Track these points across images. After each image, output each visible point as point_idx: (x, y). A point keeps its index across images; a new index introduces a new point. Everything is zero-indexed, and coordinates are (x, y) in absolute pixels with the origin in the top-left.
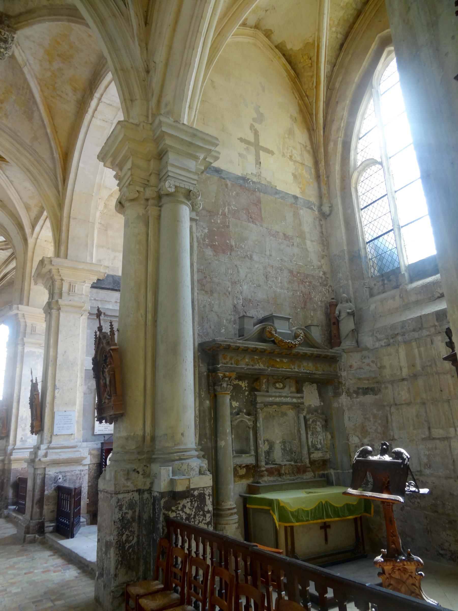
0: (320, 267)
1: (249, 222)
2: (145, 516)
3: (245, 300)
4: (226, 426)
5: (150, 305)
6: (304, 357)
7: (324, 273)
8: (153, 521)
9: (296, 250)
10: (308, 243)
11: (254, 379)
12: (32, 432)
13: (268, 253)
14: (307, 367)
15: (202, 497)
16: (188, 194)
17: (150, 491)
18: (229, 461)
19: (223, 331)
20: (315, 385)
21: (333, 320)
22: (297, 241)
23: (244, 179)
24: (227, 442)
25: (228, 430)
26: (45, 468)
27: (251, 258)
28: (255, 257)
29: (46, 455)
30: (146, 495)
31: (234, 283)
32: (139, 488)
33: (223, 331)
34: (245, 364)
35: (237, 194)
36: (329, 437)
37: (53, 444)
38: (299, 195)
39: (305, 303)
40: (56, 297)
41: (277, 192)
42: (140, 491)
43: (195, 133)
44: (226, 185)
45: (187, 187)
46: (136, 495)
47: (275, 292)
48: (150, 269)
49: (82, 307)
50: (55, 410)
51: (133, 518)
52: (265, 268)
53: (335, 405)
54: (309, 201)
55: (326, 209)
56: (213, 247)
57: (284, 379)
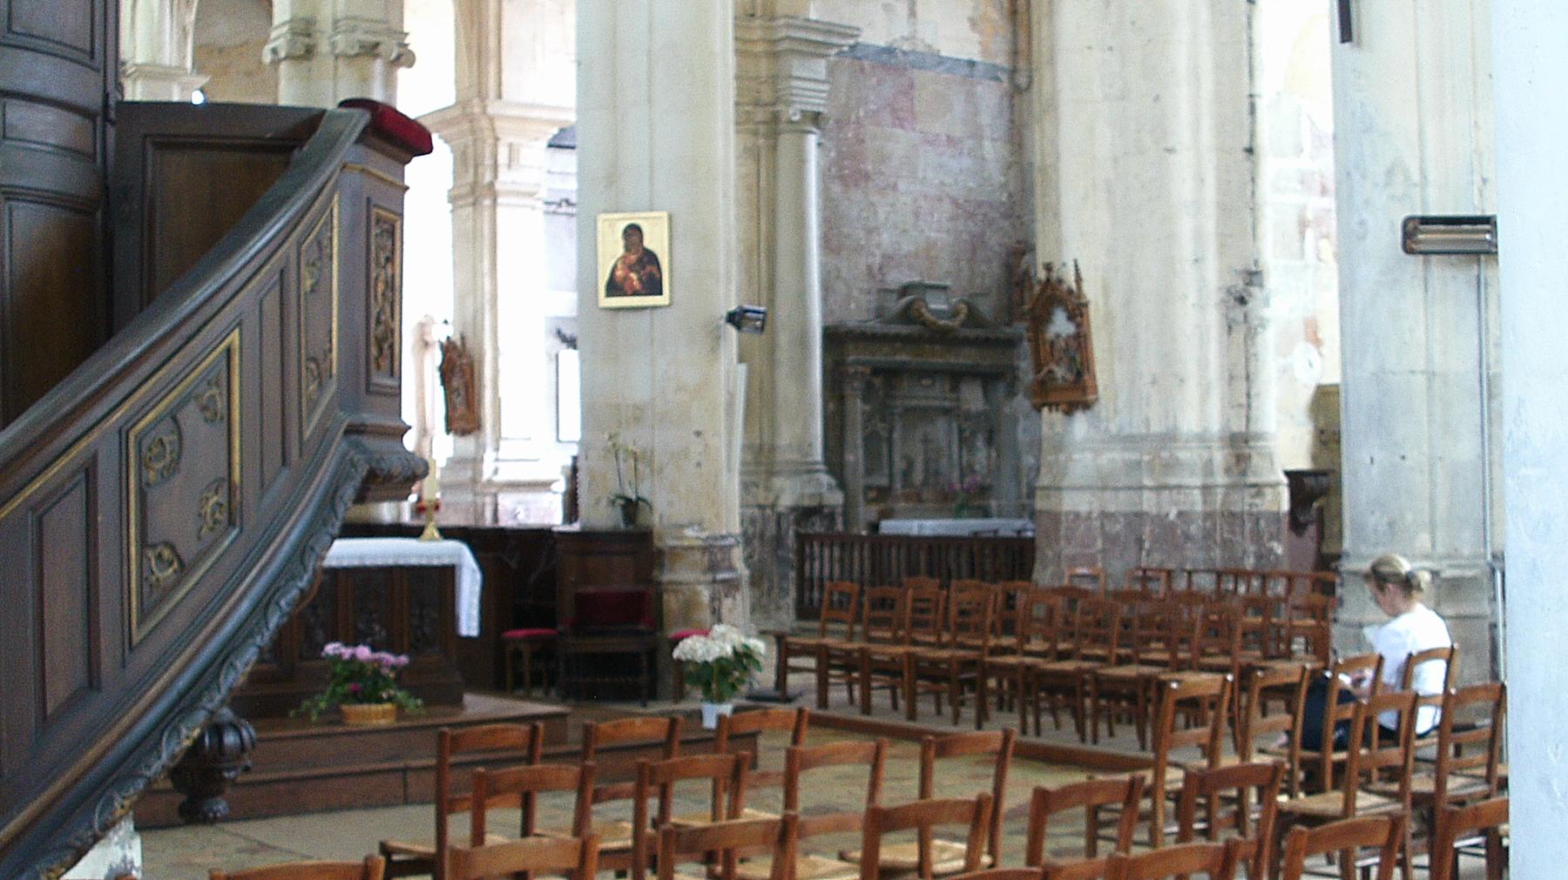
0: (1004, 186)
1: (894, 125)
2: (768, 534)
3: (884, 256)
4: (856, 437)
5: (764, 279)
6: (967, 342)
7: (1010, 196)
8: (779, 540)
9: (966, 162)
10: (987, 144)
11: (891, 374)
12: (448, 431)
13: (920, 175)
14: (964, 358)
15: (831, 517)
16: (816, 118)
17: (773, 506)
18: (858, 480)
19: (853, 306)
20: (978, 382)
21: (1016, 279)
22: (969, 143)
23: (890, 51)
24: (855, 456)
25: (859, 441)
26: (495, 495)
27: (895, 187)
28: (902, 186)
29: (496, 472)
30: (768, 511)
31: (870, 232)
32: (761, 501)
33: (853, 306)
34: (883, 356)
35: (879, 83)
36: (994, 454)
37: (501, 455)
38: (976, 58)
39: (974, 251)
40: (488, 178)
41: (941, 61)
42: (761, 507)
43: (830, 29)
44: (862, 70)
45: (816, 109)
46: (756, 512)
47: (928, 238)
48: (763, 226)
49: (531, 195)
50: (501, 394)
51: (754, 535)
52: (915, 201)
53: (1007, 410)
54: (994, 66)
55: (1022, 80)
56: (842, 178)
57: (933, 373)
